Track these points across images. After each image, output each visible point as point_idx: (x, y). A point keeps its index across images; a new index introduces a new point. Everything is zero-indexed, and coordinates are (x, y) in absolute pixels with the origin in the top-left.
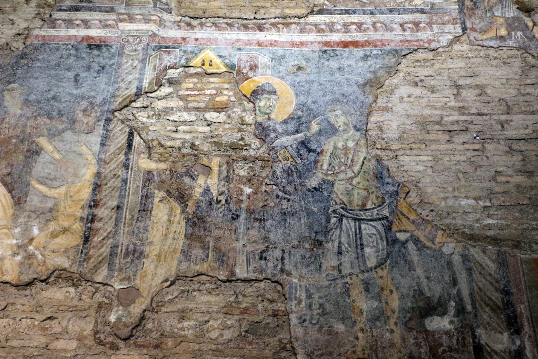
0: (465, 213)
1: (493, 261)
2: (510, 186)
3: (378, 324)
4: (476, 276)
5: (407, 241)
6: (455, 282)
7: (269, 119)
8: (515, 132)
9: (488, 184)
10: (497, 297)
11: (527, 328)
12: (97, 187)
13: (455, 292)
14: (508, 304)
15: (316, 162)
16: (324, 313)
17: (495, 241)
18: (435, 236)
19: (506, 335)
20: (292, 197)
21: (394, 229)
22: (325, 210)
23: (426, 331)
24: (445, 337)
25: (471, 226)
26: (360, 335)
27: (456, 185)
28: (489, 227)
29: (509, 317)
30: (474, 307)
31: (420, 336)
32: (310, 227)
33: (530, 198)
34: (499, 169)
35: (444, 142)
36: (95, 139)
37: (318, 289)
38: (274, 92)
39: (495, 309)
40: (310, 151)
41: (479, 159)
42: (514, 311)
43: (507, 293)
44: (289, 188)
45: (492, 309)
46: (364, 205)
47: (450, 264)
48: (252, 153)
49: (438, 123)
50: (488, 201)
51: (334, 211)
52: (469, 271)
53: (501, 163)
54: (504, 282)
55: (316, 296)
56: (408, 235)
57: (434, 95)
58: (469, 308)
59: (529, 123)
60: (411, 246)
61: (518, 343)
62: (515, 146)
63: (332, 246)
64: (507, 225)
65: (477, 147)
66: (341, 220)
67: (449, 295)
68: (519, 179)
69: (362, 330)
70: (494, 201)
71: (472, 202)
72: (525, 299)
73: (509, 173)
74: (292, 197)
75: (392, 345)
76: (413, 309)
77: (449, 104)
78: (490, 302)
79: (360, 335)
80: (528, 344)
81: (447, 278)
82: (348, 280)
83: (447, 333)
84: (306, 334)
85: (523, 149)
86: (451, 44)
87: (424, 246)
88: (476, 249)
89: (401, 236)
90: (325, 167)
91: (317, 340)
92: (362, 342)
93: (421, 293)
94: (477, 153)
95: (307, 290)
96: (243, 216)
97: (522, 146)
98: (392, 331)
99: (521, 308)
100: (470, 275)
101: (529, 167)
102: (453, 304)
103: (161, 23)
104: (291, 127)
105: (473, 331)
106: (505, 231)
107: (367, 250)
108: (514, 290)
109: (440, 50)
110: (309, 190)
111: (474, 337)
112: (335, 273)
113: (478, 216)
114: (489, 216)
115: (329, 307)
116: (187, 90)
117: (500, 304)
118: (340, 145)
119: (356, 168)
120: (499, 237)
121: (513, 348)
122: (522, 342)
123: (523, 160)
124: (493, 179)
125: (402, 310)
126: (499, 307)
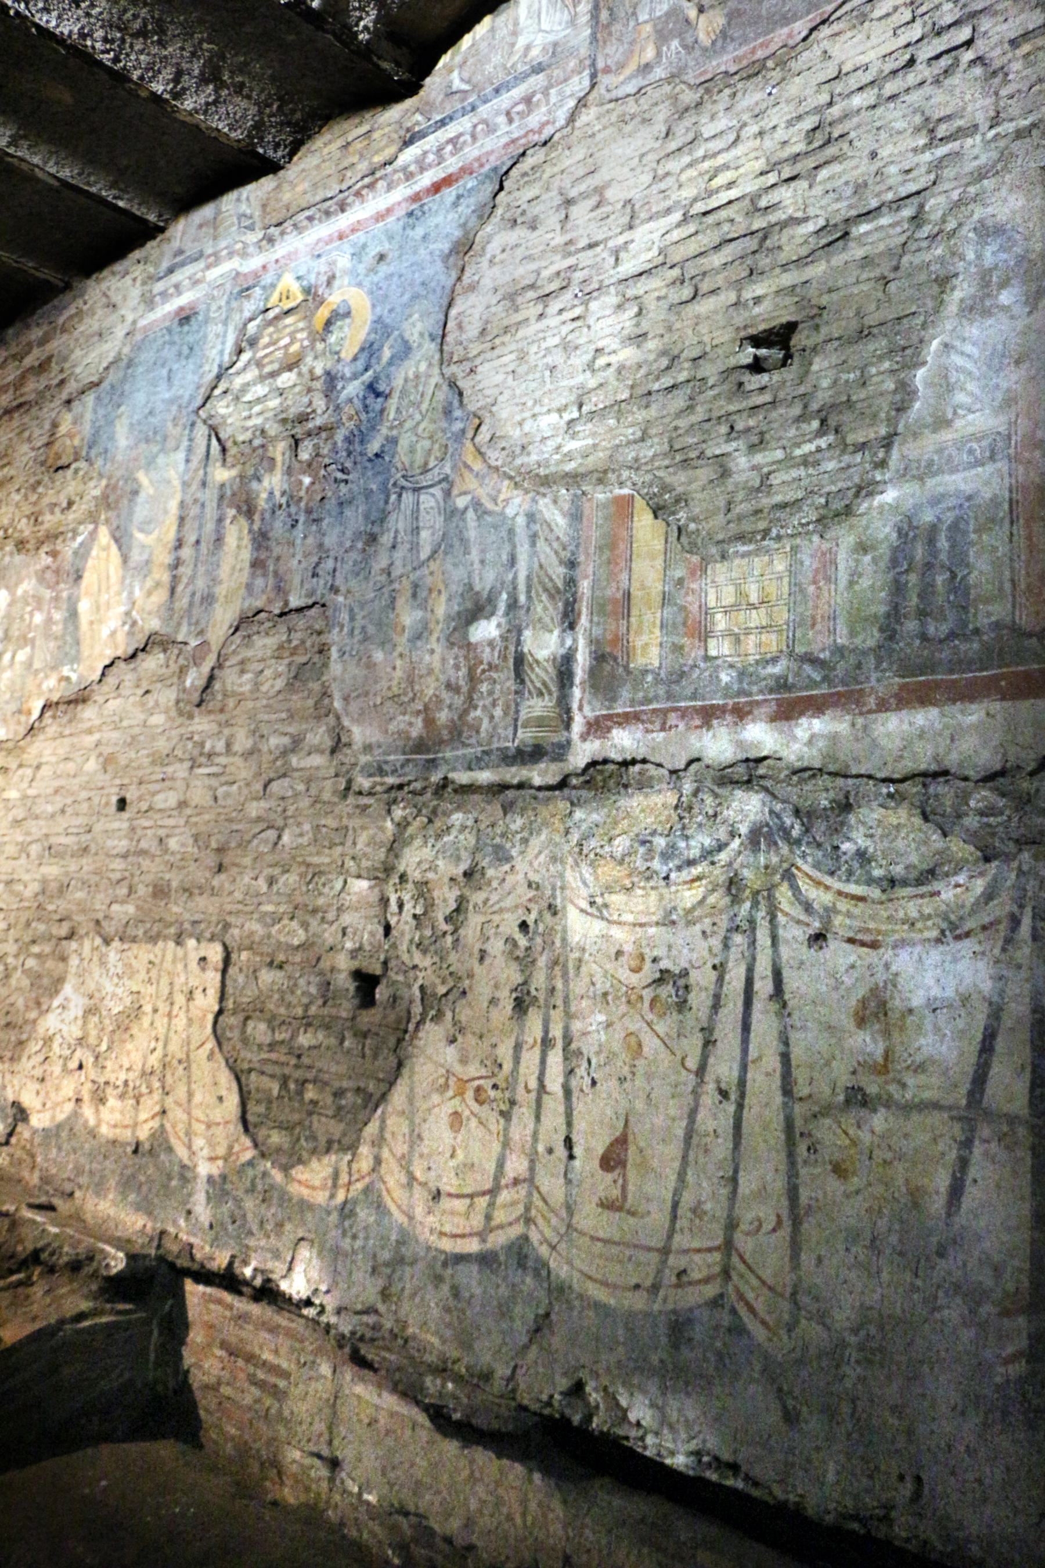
0: (544, 439)
1: (564, 515)
2: (612, 369)
3: (419, 643)
4: (541, 544)
5: (466, 508)
6: (513, 561)
7: (339, 360)
8: (633, 262)
9: (580, 378)
10: (558, 573)
11: (584, 621)
12: (182, 520)
13: (510, 576)
14: (571, 582)
15: (382, 411)
16: (366, 639)
17: (573, 479)
18: (499, 491)
19: (556, 633)
20: (350, 477)
21: (455, 492)
22: (384, 484)
23: (469, 644)
24: (488, 650)
25: (547, 460)
26: (399, 663)
27: (538, 394)
28: (569, 457)
29: (567, 604)
30: (529, 598)
31: (462, 653)
32: (366, 517)
33: (632, 387)
34: (600, 344)
35: (533, 320)
36: (181, 455)
37: (362, 605)
38: (348, 314)
39: (553, 594)
40: (378, 395)
41: (577, 334)
42: (574, 594)
43: (572, 564)
44: (348, 465)
45: (552, 597)
46: (426, 464)
47: (511, 532)
48: (319, 422)
49: (532, 286)
50: (575, 409)
51: (395, 484)
52: (534, 538)
53: (608, 331)
54: (572, 548)
55: (359, 617)
56: (469, 497)
57: (537, 233)
58: (522, 599)
59: (656, 236)
60: (471, 514)
61: (569, 642)
62: (630, 293)
63: (386, 539)
64: (595, 446)
65: (577, 312)
66: (400, 496)
67: (503, 583)
68: (628, 354)
69: (401, 655)
70: (585, 409)
71: (554, 417)
72: (590, 570)
73: (614, 346)
74: (350, 477)
75: (430, 671)
76: (459, 613)
77: (553, 243)
78: (550, 585)
79: (399, 663)
80: (582, 643)
81: (504, 557)
82: (396, 586)
83: (491, 643)
84: (345, 670)
85: (641, 292)
86: (572, 118)
87: (486, 512)
88: (547, 500)
89: (461, 502)
90: (391, 417)
91: (354, 678)
92: (399, 673)
93: (471, 588)
94: (578, 323)
95: (351, 610)
96: (302, 519)
97: (639, 288)
98: (432, 652)
99: (585, 586)
100: (533, 544)
101: (645, 326)
102: (504, 596)
103: (244, 254)
104: (360, 365)
105: (520, 632)
106: (591, 458)
107: (424, 534)
108: (582, 558)
109: (556, 138)
110: (370, 460)
111: (518, 643)
112: (383, 578)
113: (559, 440)
114: (574, 436)
115: (371, 630)
116: (266, 346)
117: (560, 584)
118: (411, 375)
119: (424, 406)
120: (582, 470)
121: (562, 651)
122: (575, 640)
123: (639, 314)
124: (590, 366)
125: (449, 618)
126: (558, 591)
